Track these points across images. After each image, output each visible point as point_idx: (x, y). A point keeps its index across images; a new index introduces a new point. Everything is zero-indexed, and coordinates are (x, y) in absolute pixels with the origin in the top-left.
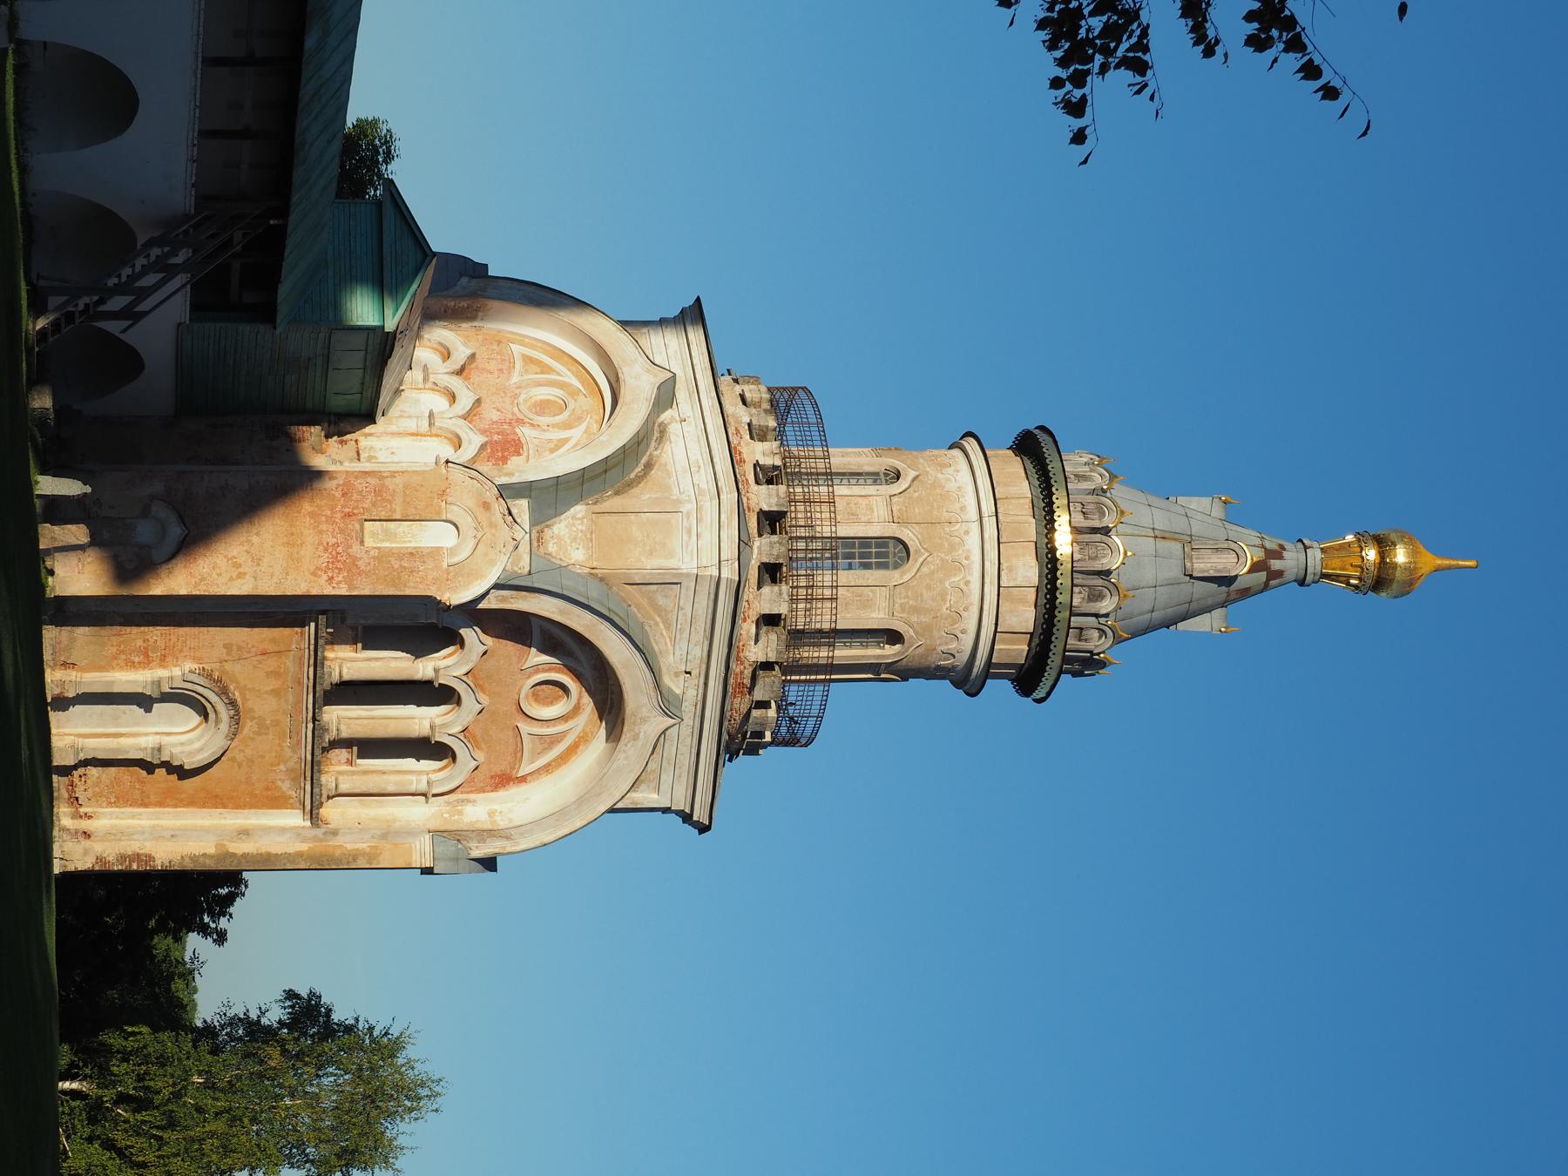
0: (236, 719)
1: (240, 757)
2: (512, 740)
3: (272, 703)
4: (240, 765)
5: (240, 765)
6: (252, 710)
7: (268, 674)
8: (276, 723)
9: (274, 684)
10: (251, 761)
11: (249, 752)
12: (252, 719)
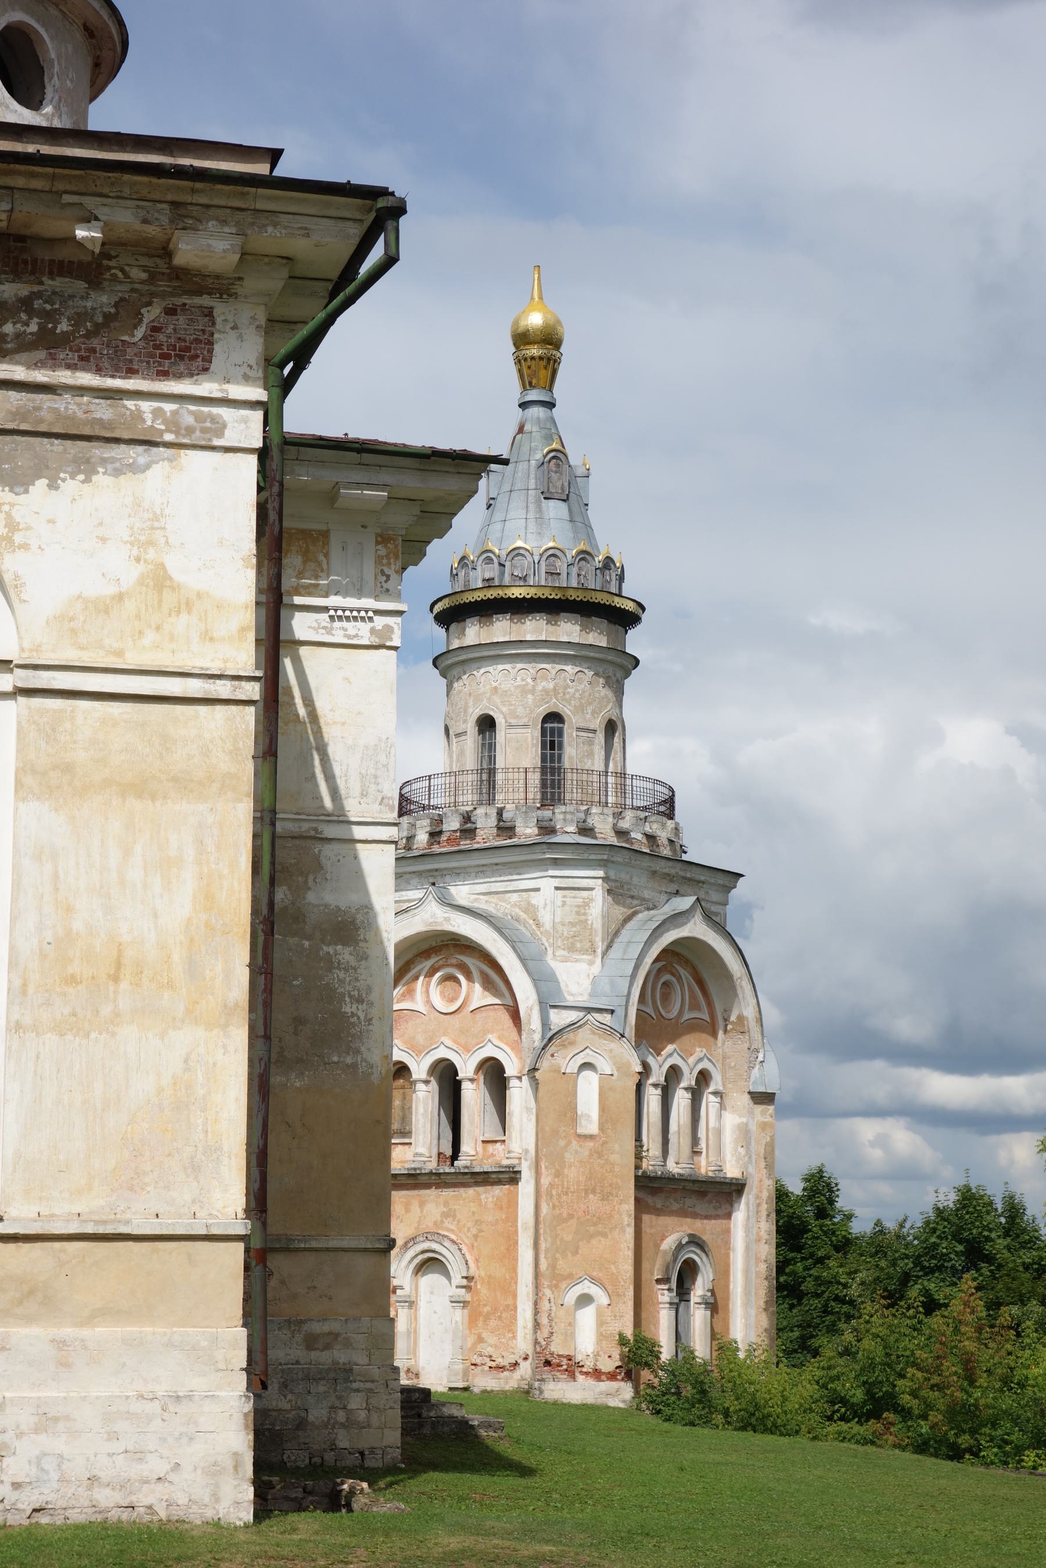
0: (427, 1236)
1: (474, 1231)
2: (484, 1014)
3: (430, 1207)
4: (481, 1231)
5: (481, 1231)
6: (435, 1223)
7: (407, 1210)
8: (446, 1204)
9: (415, 1207)
10: (478, 1222)
11: (469, 1224)
12: (442, 1222)
